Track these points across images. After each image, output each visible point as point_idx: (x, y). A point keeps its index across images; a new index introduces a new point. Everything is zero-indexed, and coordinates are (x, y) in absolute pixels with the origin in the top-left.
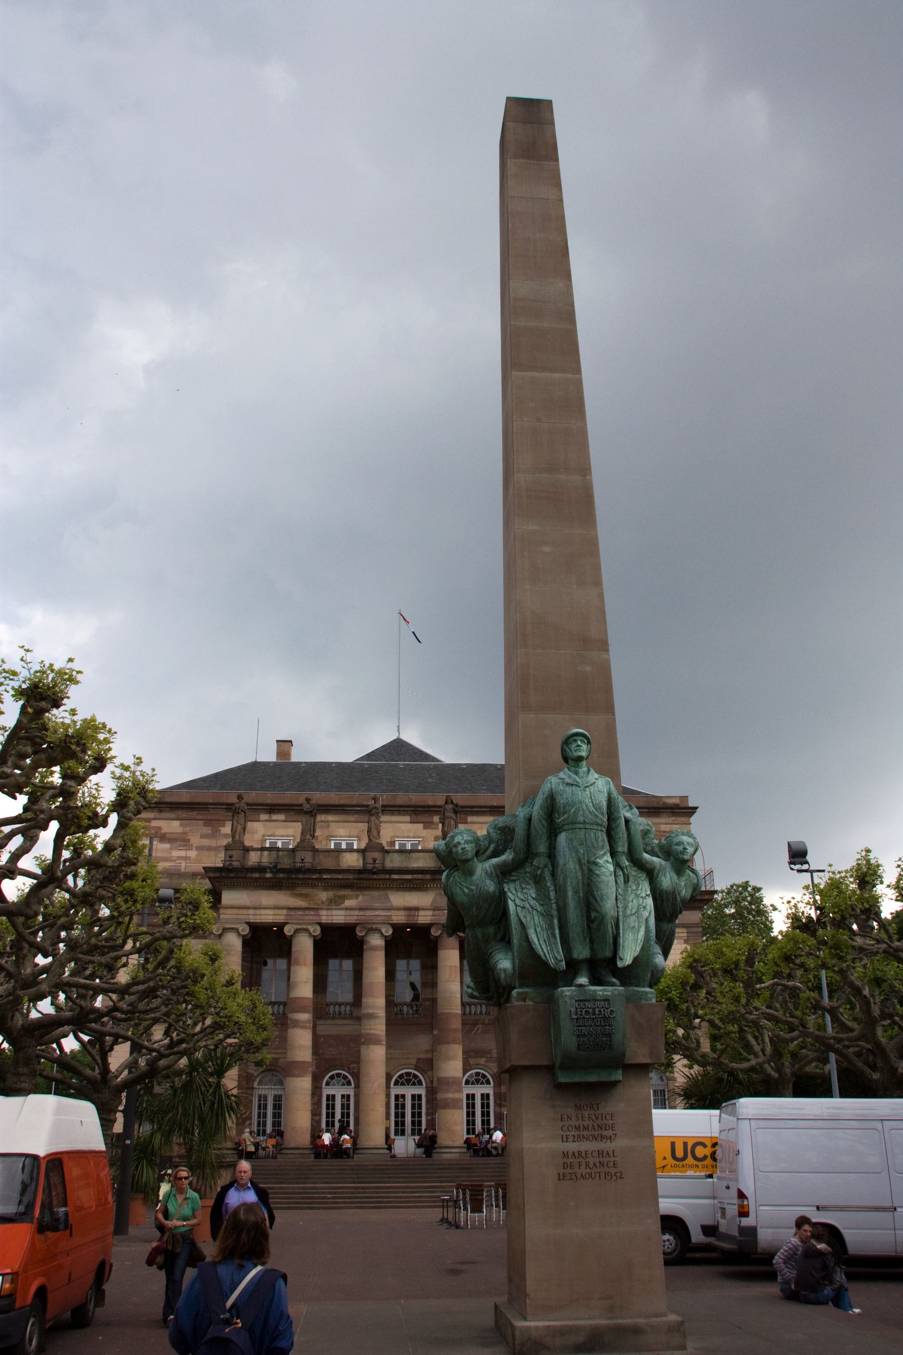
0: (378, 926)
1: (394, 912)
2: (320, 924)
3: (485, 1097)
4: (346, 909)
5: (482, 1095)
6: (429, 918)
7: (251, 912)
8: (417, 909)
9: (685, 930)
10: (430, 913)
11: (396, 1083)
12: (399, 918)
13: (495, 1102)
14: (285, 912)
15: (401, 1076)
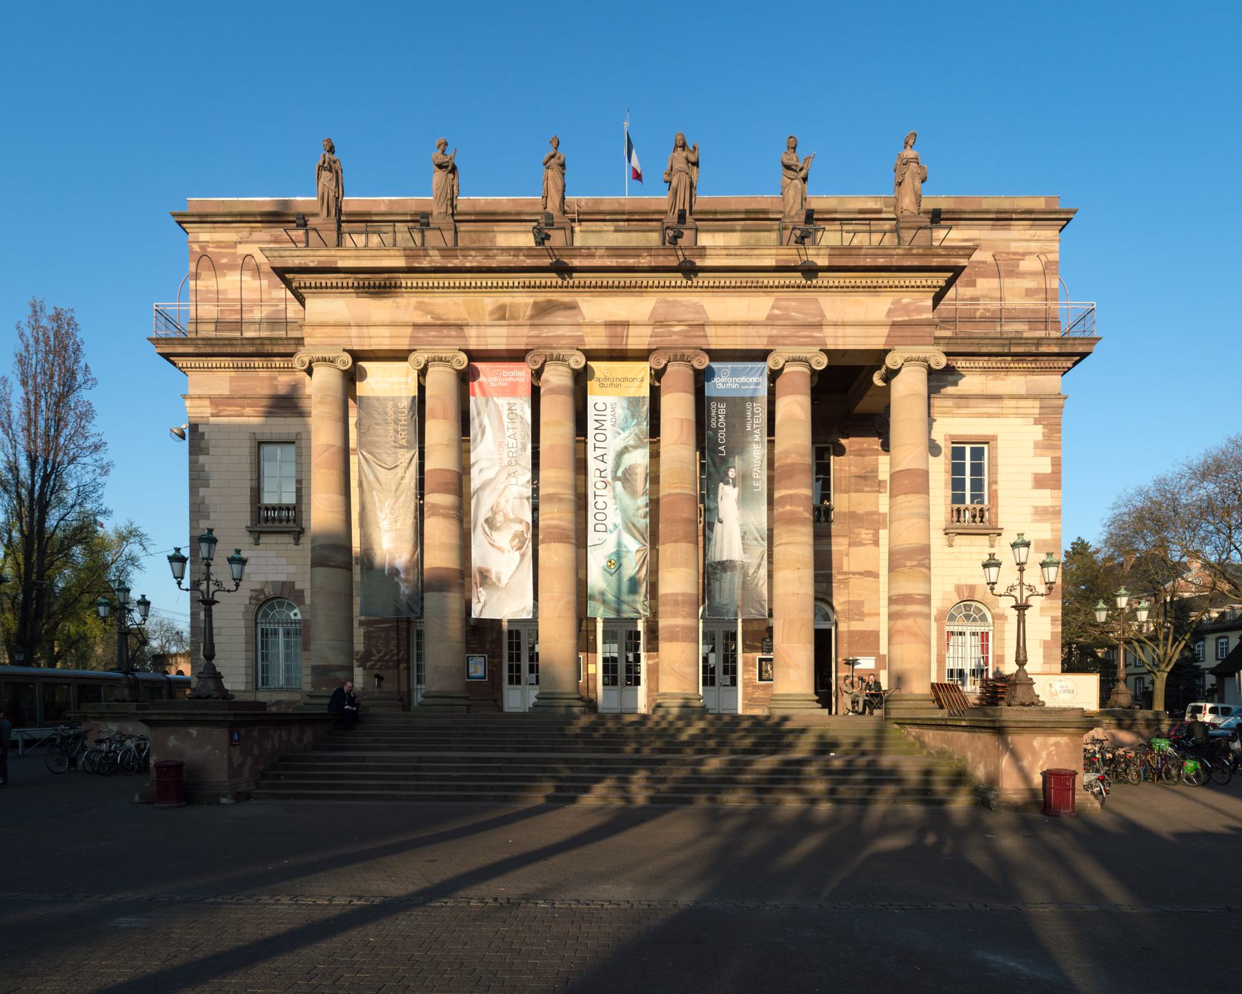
0: (563, 352)
1: (587, 329)
2: (467, 352)
6: (647, 340)
7: (354, 331)
8: (626, 324)
9: (1037, 403)
10: (648, 331)
12: (597, 340)
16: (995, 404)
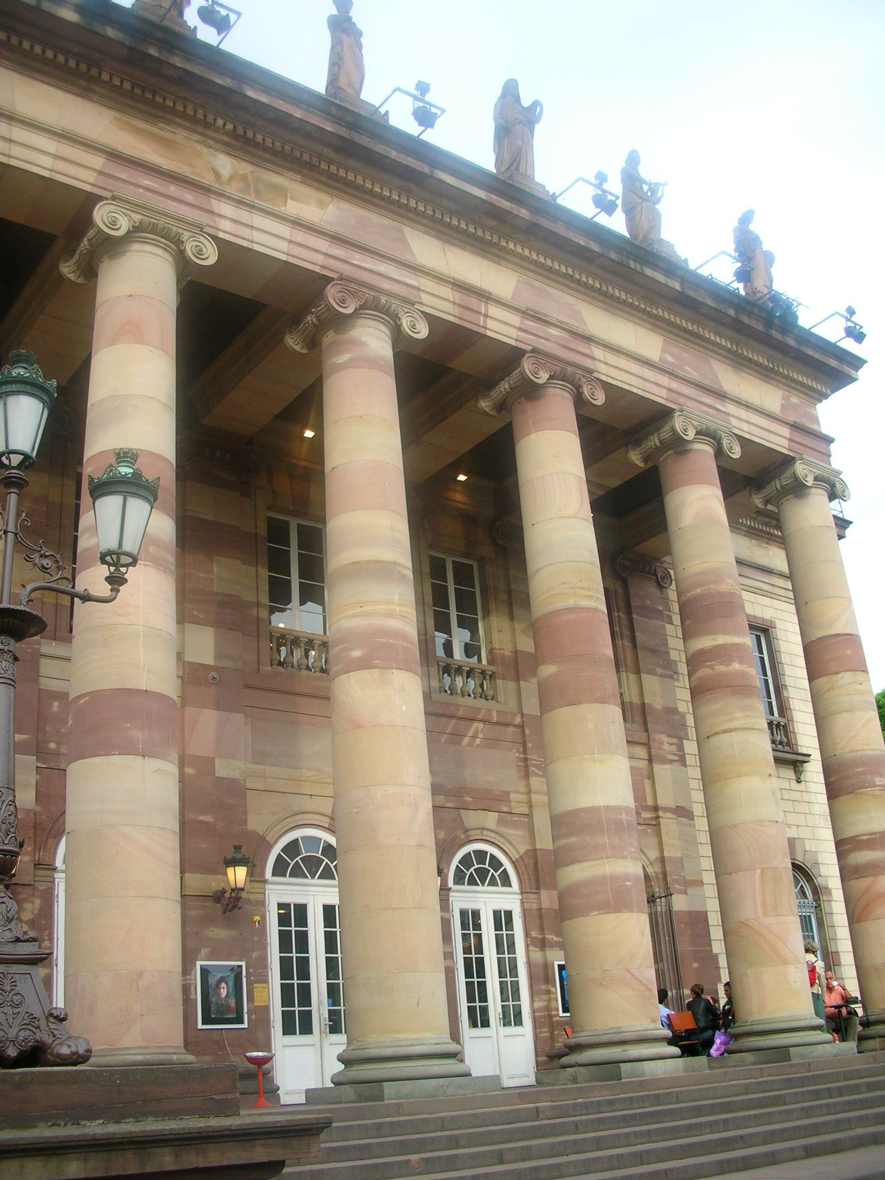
3: (503, 919)
4: (297, 223)
5: (497, 914)
8: (485, 296)
11: (280, 869)
12: (443, 304)
13: (527, 934)
14: (97, 161)
15: (292, 848)
16: (766, 578)
